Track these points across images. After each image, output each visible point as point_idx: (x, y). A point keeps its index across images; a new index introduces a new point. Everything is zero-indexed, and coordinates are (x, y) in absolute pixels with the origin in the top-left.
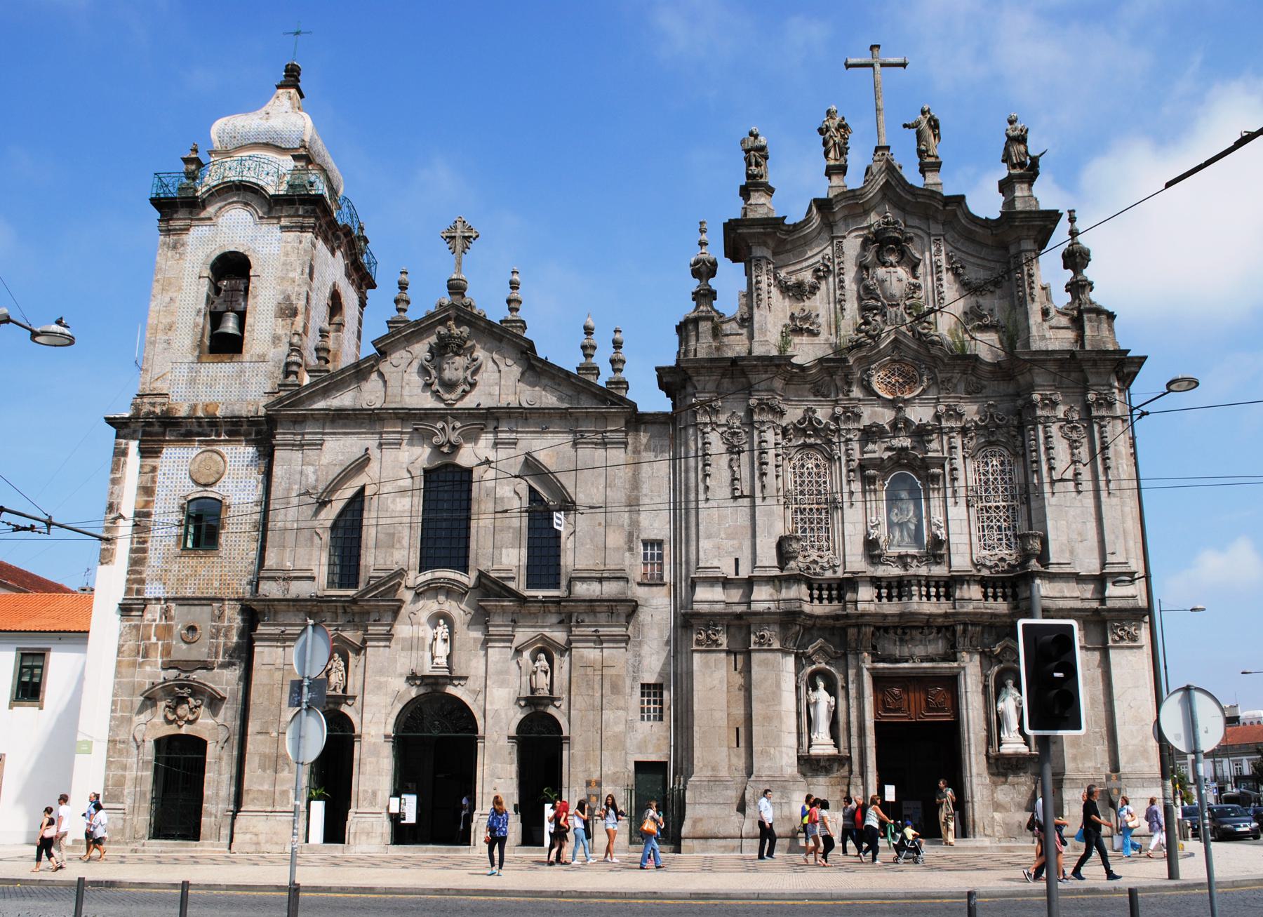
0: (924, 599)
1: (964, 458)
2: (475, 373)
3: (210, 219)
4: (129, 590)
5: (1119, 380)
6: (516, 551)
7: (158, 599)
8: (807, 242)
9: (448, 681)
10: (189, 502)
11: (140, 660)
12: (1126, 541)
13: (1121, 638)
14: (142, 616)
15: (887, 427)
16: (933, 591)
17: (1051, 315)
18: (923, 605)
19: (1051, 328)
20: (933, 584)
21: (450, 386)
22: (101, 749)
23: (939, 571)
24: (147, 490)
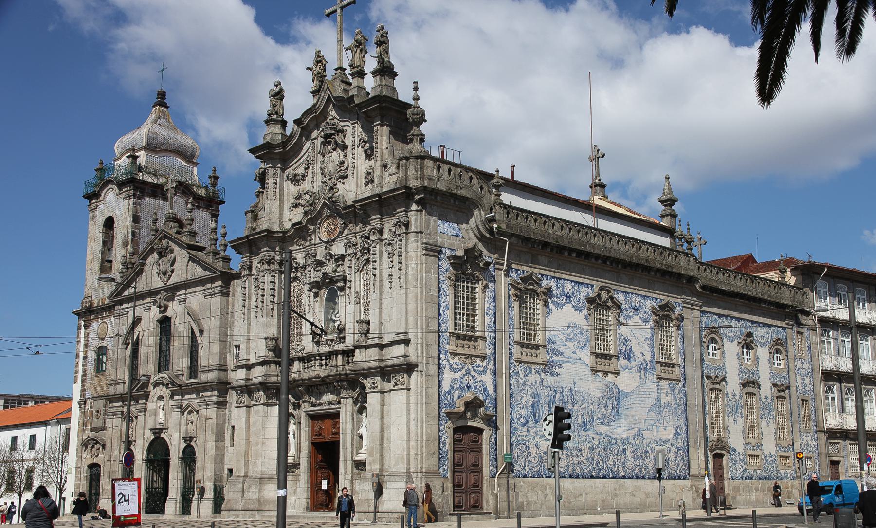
0: (318, 368)
1: (355, 272)
2: (172, 265)
3: (102, 201)
4: (81, 394)
5: (418, 203)
6: (184, 359)
7: (89, 398)
8: (299, 147)
9: (161, 431)
10: (98, 349)
11: (85, 428)
12: (406, 317)
13: (396, 384)
14: (85, 407)
15: (323, 260)
16: (323, 362)
17: (389, 166)
18: (317, 371)
19: (389, 175)
20: (324, 358)
21: (165, 274)
22: (74, 470)
23: (341, 347)
24: (86, 346)
